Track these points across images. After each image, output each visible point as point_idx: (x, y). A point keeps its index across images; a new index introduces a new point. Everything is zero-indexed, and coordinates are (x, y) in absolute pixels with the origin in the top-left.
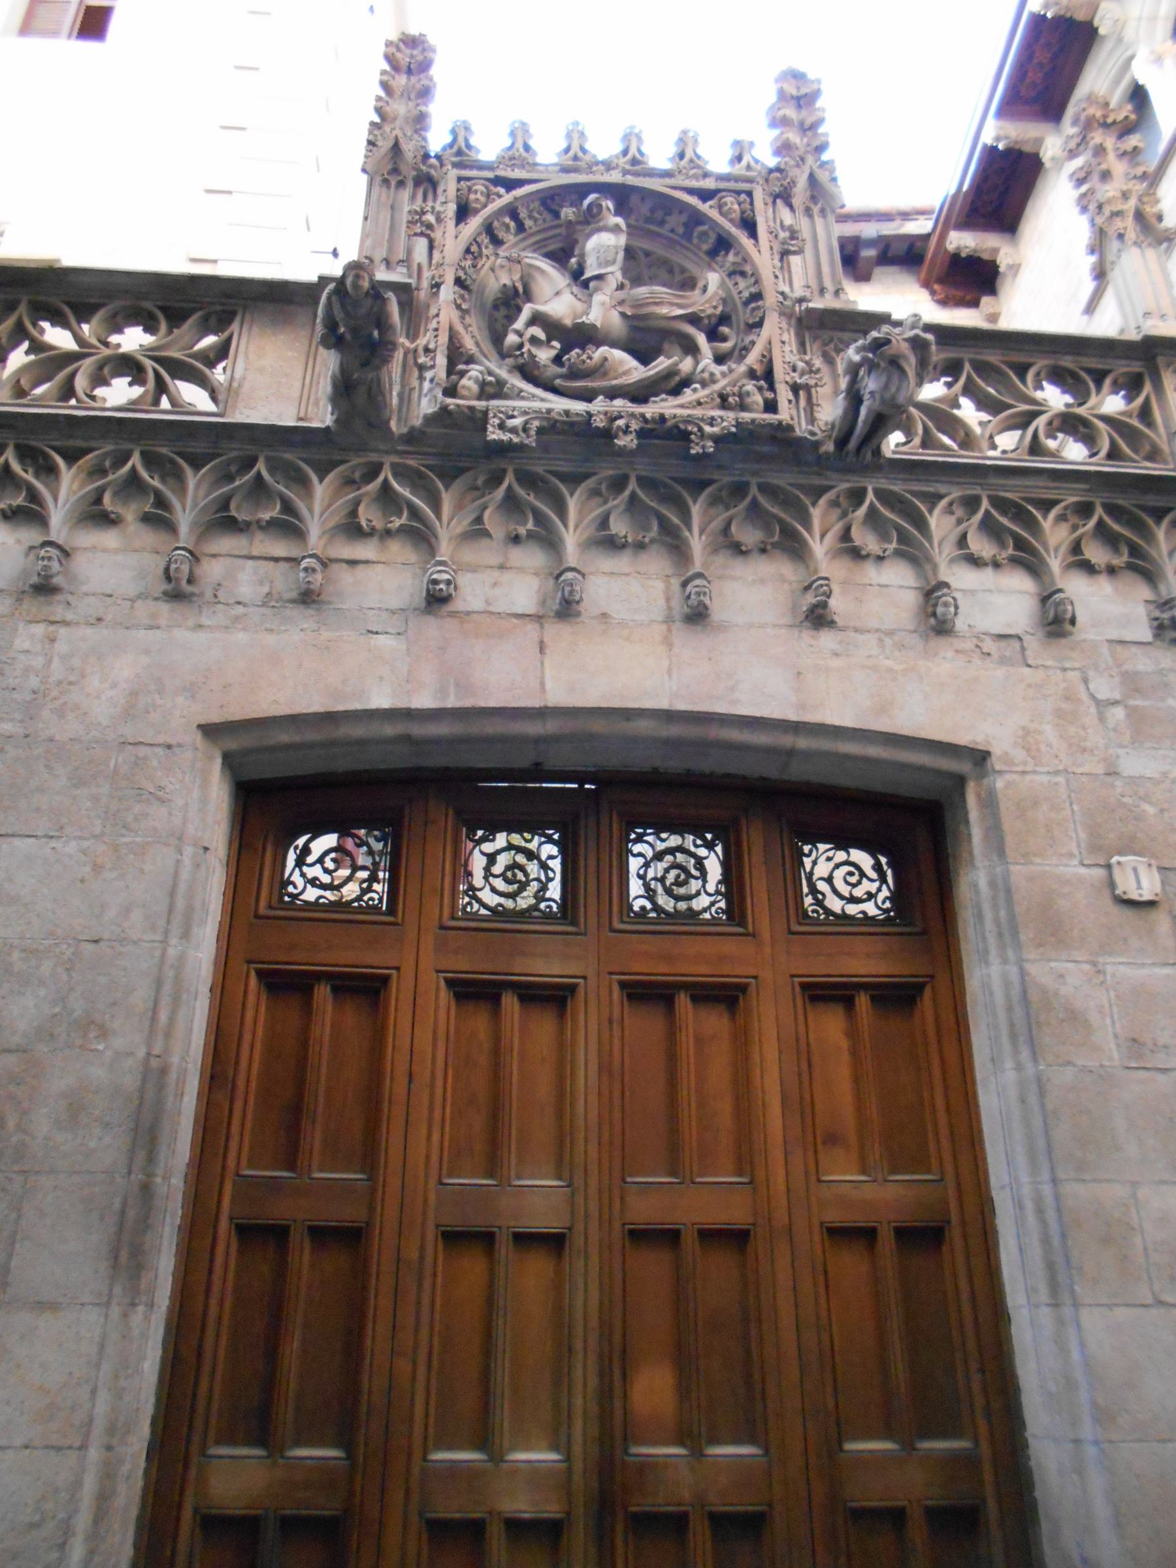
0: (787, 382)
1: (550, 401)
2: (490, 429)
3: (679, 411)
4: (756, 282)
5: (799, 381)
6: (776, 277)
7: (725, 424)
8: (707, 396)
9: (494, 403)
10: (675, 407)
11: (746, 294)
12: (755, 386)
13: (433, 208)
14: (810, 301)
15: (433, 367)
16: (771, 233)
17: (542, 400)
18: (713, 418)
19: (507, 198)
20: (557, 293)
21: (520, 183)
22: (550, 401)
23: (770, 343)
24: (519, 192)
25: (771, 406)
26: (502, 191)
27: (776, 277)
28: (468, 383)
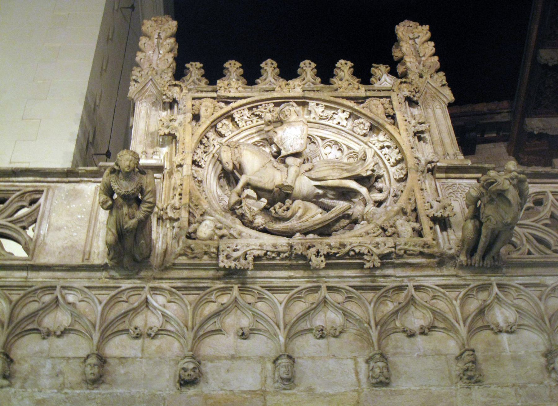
3: (353, 240)
5: (436, 215)
15: (178, 219)
19: (226, 108)
25: (419, 233)
26: (222, 105)
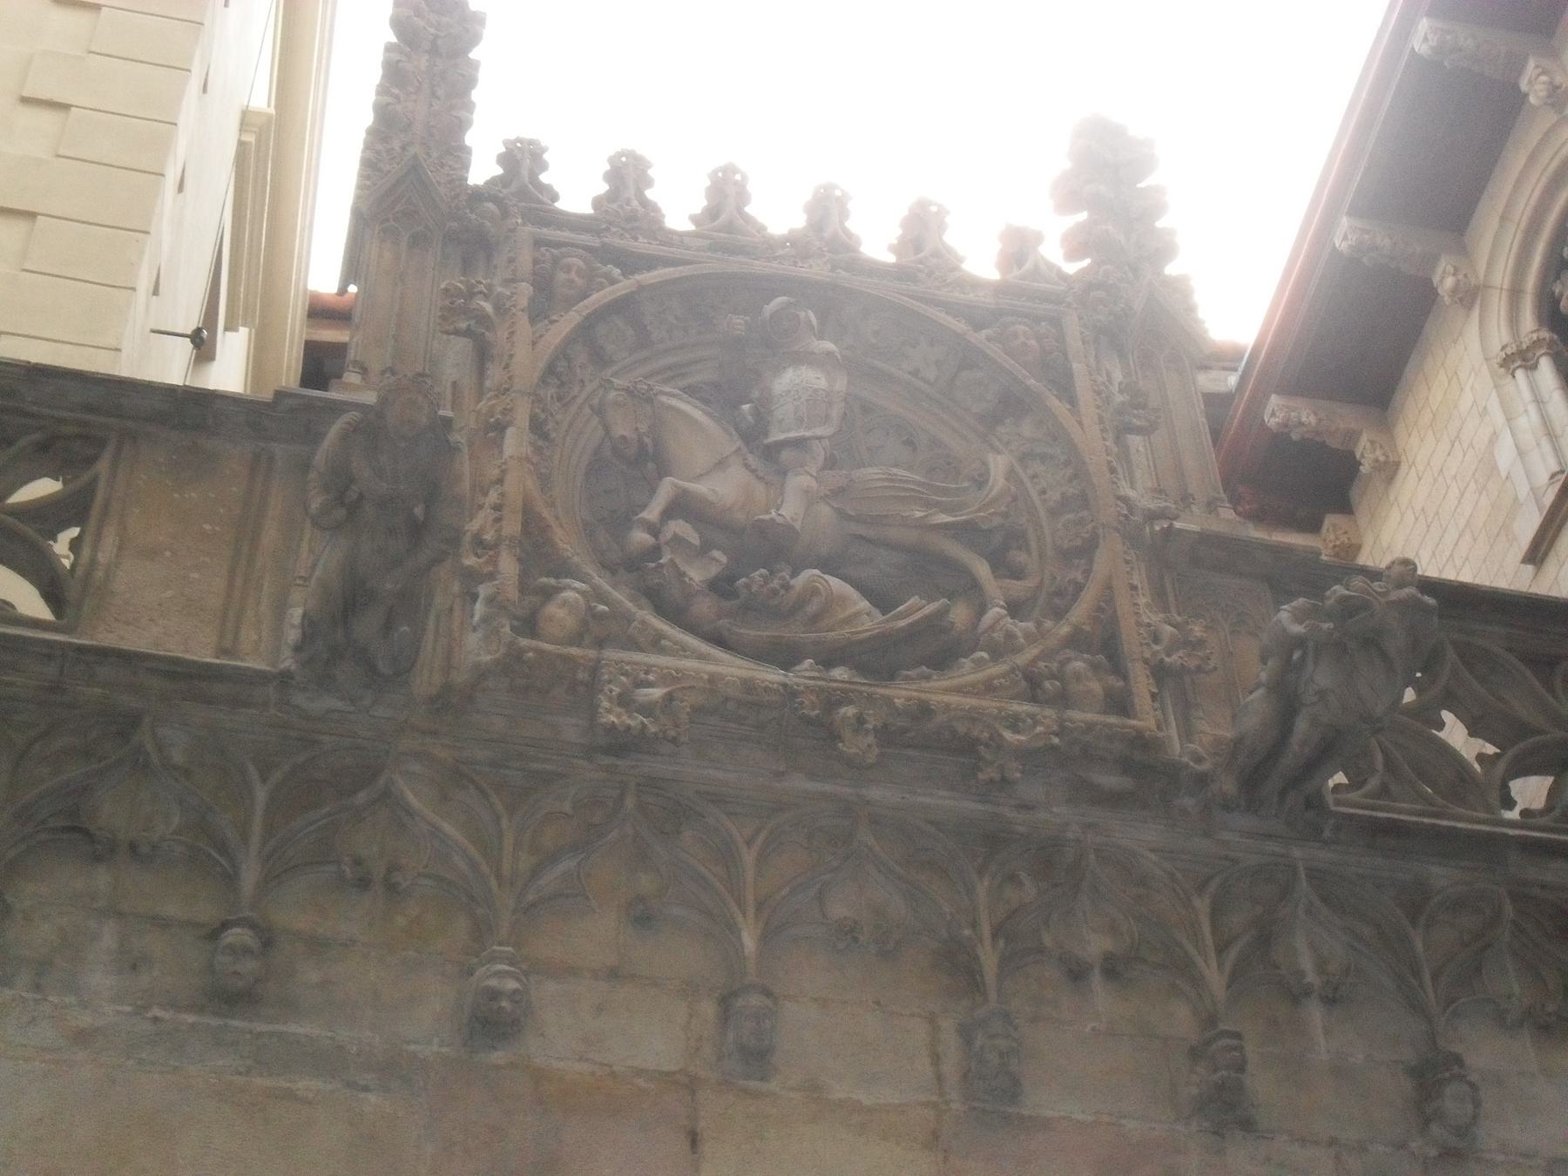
0: (1146, 661)
1: (717, 661)
2: (606, 704)
3: (953, 699)
4: (1076, 476)
6: (1113, 471)
7: (1039, 729)
8: (1004, 676)
9: (611, 654)
10: (947, 691)
11: (1054, 496)
12: (1084, 661)
13: (490, 287)
14: (1176, 518)
15: (491, 576)
16: (1099, 393)
17: (701, 657)
19: (624, 286)
20: (721, 464)
21: (651, 262)
22: (717, 661)
23: (1110, 587)
25: (1120, 704)
26: (617, 272)
27: (1113, 471)
28: (561, 612)
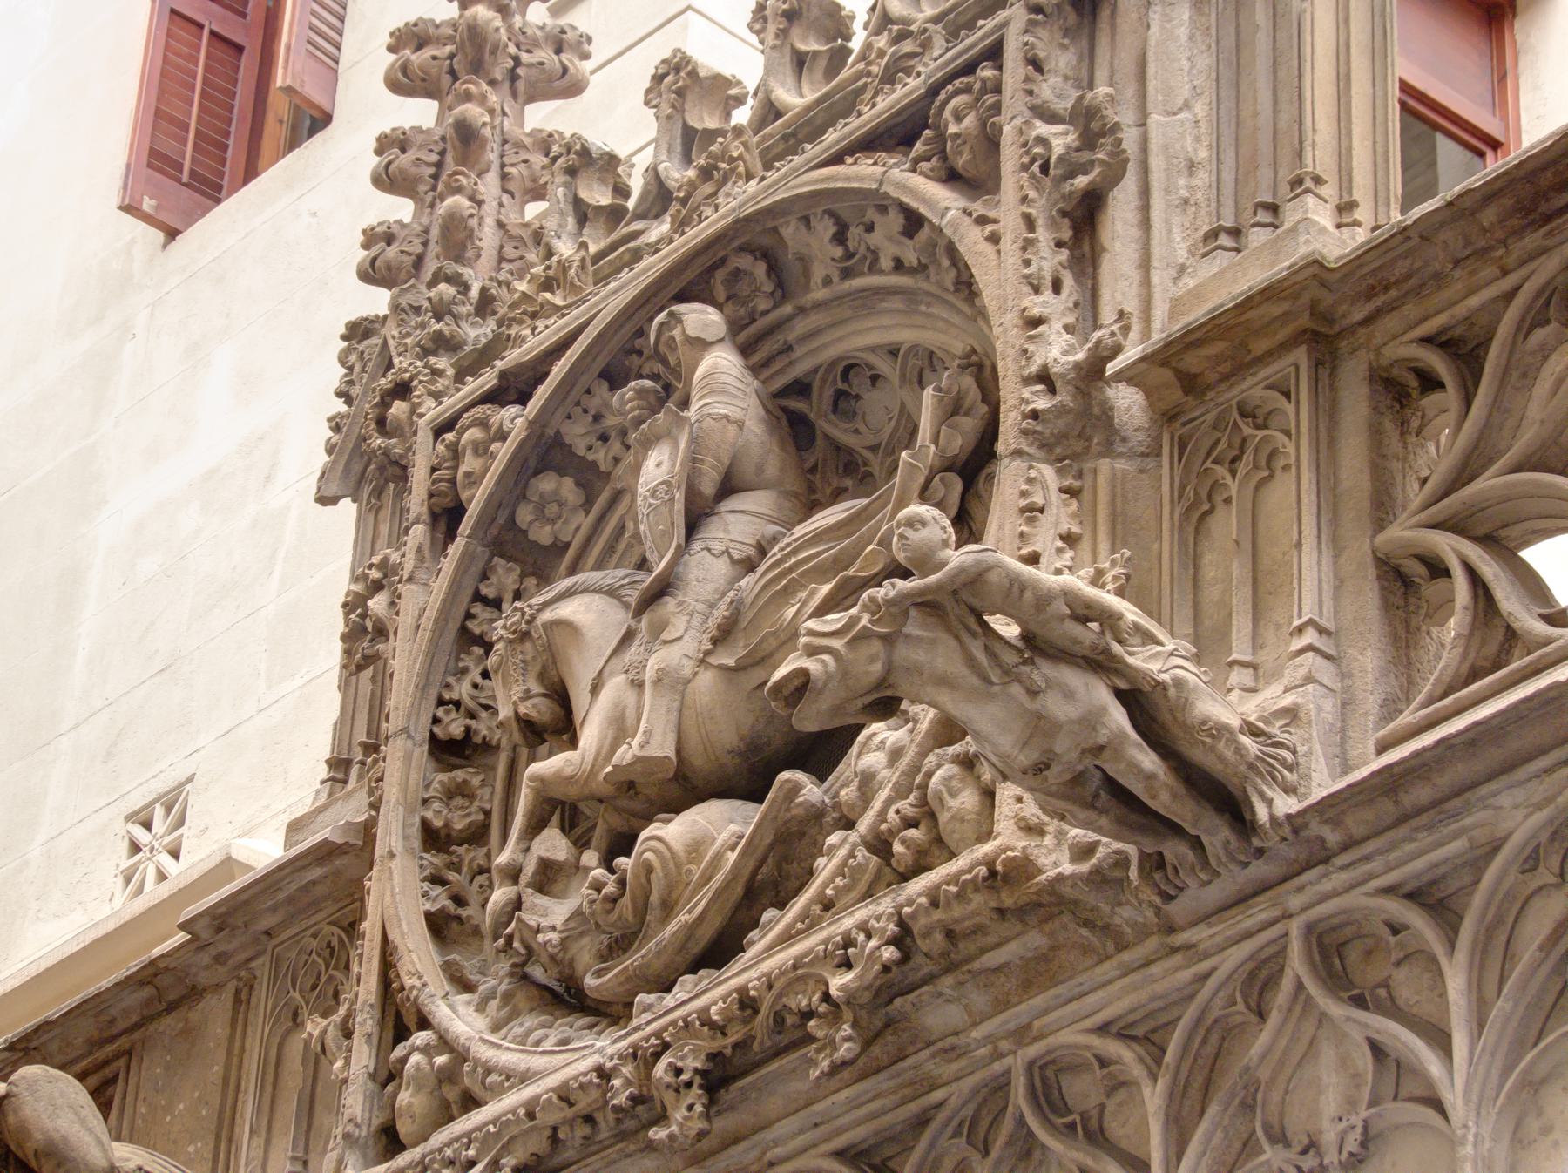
18: (848, 942)
24: (542, 393)
